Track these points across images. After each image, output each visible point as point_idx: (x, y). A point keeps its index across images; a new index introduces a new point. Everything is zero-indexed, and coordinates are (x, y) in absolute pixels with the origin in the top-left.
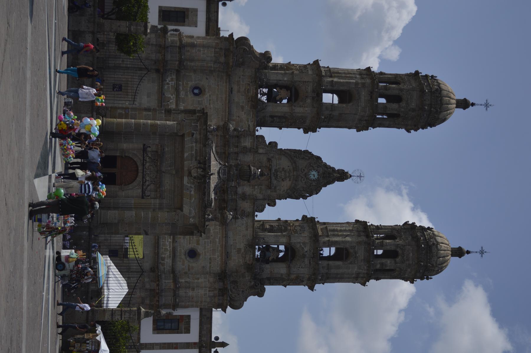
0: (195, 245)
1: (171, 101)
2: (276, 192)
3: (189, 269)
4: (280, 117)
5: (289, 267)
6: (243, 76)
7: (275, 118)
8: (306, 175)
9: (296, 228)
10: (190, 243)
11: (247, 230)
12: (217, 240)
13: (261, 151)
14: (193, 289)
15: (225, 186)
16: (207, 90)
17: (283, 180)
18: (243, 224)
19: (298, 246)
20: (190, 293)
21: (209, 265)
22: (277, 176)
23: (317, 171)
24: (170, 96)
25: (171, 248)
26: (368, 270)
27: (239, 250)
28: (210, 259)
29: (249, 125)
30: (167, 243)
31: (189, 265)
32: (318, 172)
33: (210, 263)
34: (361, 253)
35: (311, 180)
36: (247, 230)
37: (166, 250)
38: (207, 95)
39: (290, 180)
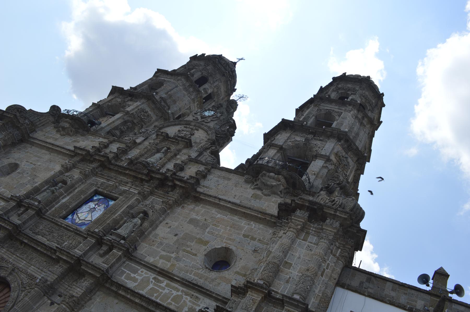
0: (205, 247)
3: (245, 275)
10: (196, 255)
11: (229, 179)
12: (219, 216)
13: (138, 141)
14: (288, 265)
18: (218, 181)
20: (294, 273)
21: (256, 243)
25: (181, 288)
26: (354, 106)
27: (255, 197)
28: (245, 236)
30: (166, 291)
31: (237, 273)
33: (253, 239)
37: (176, 299)
39: (198, 130)
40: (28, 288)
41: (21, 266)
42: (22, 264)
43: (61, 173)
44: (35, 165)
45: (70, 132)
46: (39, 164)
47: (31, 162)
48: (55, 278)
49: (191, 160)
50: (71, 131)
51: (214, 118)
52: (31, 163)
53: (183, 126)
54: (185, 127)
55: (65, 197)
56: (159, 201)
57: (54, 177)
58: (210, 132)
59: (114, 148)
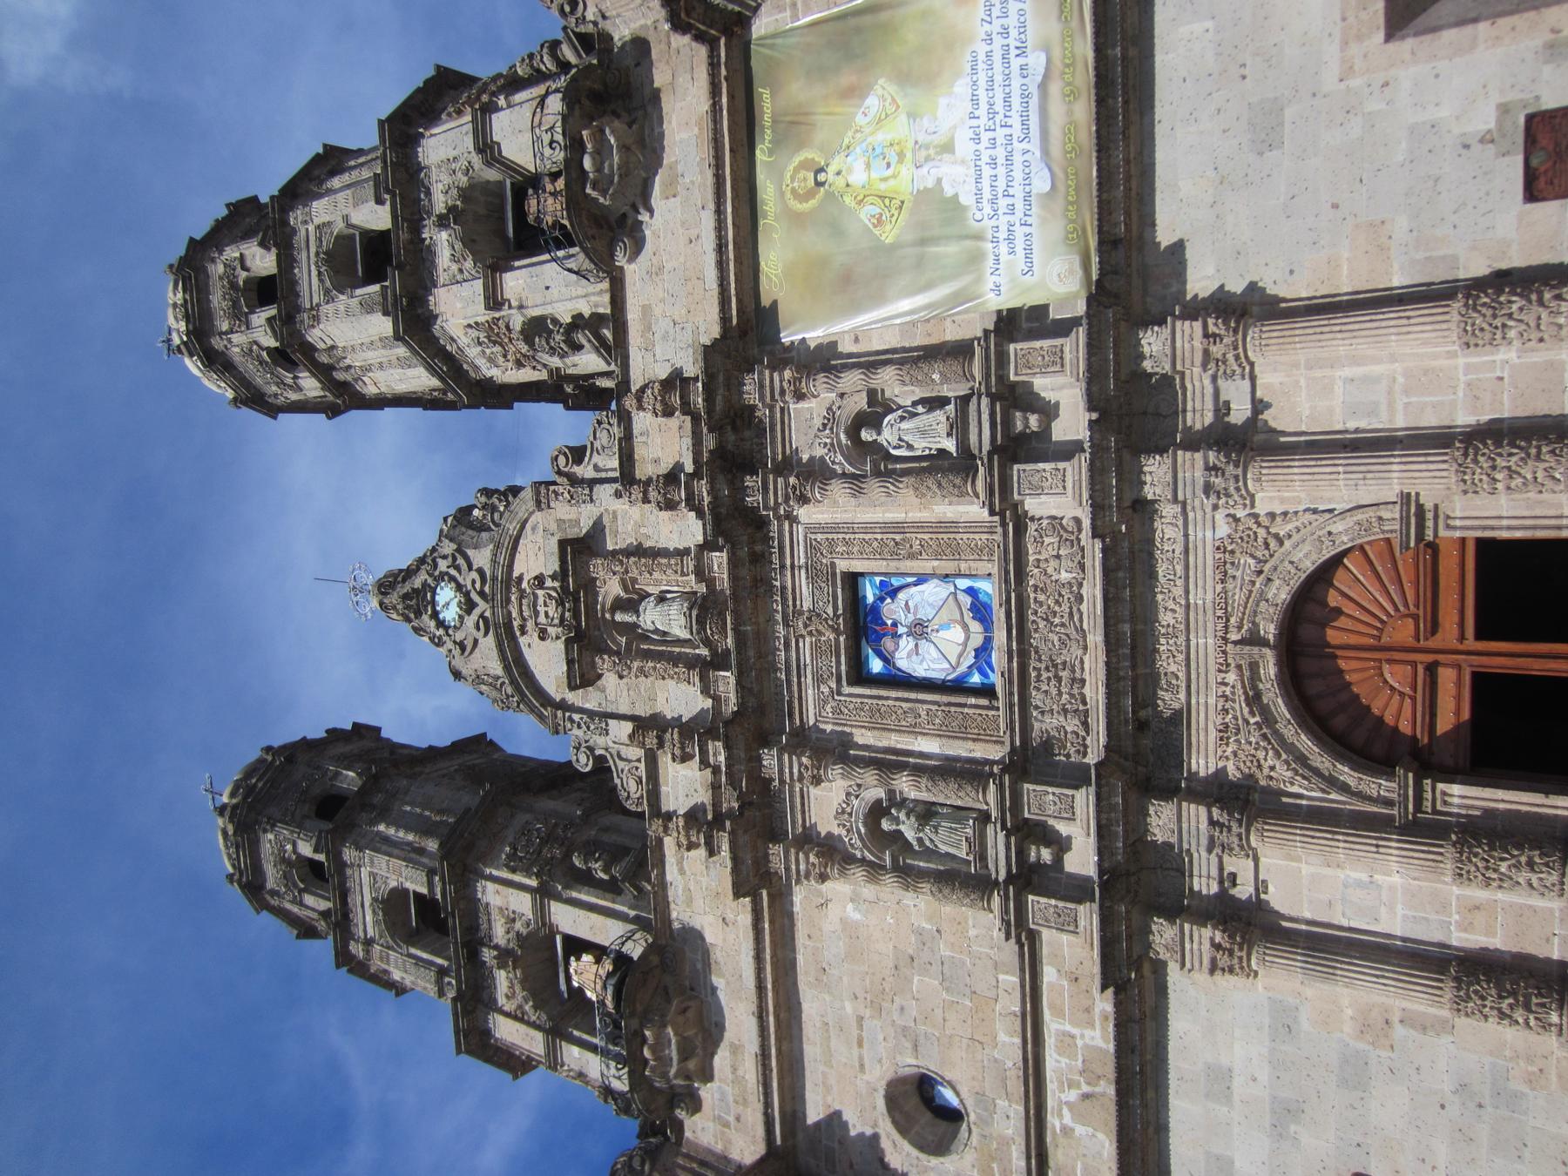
1: (1072, 1095)
2: (560, 522)
4: (585, 879)
5: (487, 148)
6: (726, 1125)
7: (602, 875)
8: (469, 606)
9: (497, 349)
11: (646, 310)
15: (744, 552)
16: (881, 1103)
17: (540, 580)
18: (665, 337)
19: (469, 264)
22: (560, 603)
23: (441, 624)
24: (1080, 1130)
29: (682, 871)
32: (435, 615)
34: (310, 279)
35: (452, 579)
36: (646, 310)
38: (878, 1076)
39: (520, 578)
40: (1262, 533)
41: (1210, 641)
42: (1205, 643)
43: (848, 860)
44: (860, 1019)
45: (690, 1014)
46: (849, 1007)
47: (855, 1052)
48: (1188, 454)
49: (627, 477)
50: (684, 1011)
51: (459, 571)
52: (860, 1044)
53: (523, 641)
54: (523, 633)
55: (922, 755)
56: (797, 430)
57: (874, 870)
58: (512, 528)
59: (684, 784)
